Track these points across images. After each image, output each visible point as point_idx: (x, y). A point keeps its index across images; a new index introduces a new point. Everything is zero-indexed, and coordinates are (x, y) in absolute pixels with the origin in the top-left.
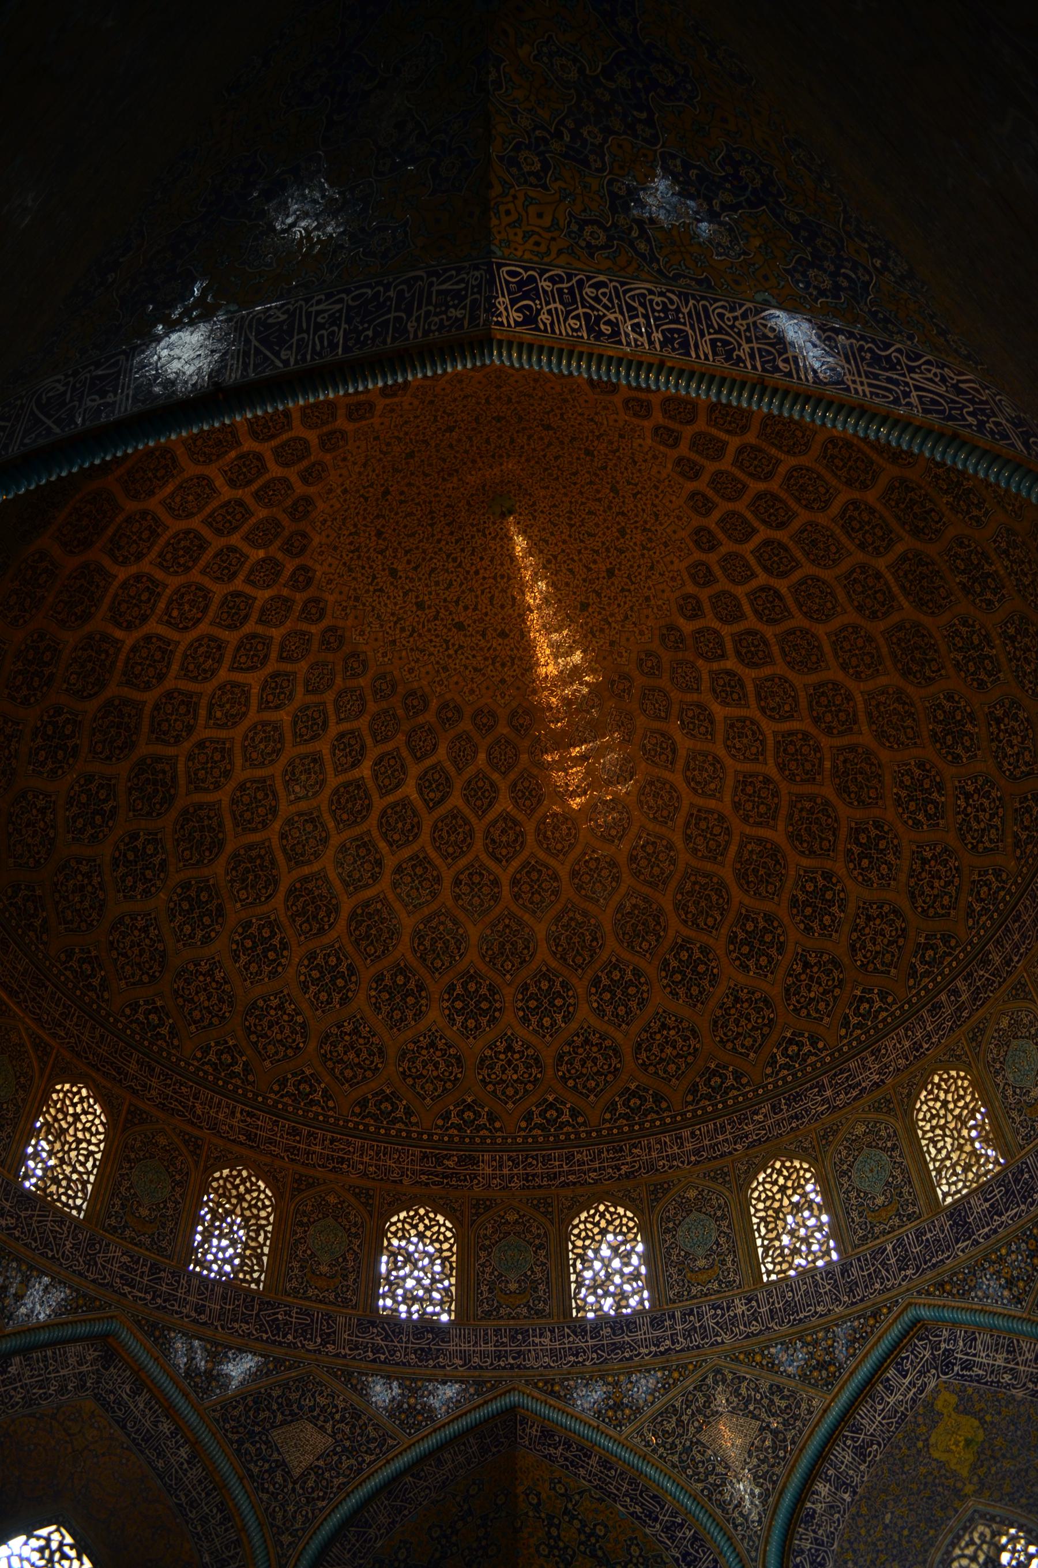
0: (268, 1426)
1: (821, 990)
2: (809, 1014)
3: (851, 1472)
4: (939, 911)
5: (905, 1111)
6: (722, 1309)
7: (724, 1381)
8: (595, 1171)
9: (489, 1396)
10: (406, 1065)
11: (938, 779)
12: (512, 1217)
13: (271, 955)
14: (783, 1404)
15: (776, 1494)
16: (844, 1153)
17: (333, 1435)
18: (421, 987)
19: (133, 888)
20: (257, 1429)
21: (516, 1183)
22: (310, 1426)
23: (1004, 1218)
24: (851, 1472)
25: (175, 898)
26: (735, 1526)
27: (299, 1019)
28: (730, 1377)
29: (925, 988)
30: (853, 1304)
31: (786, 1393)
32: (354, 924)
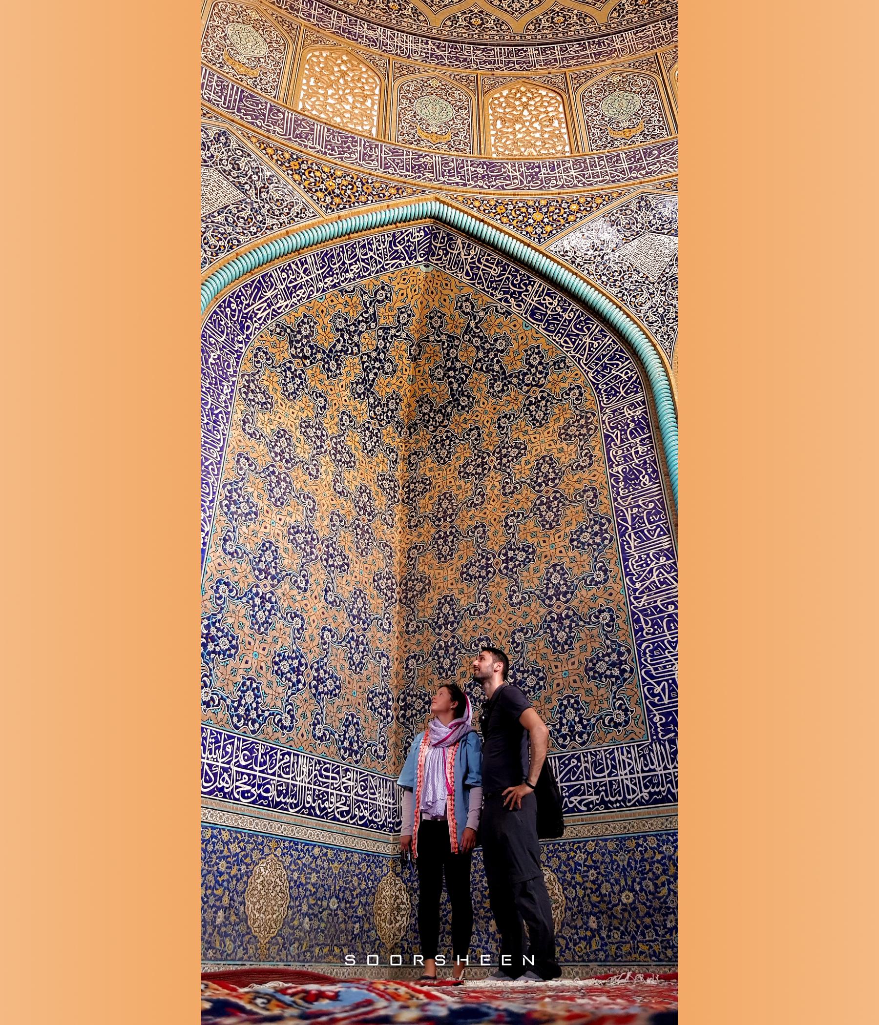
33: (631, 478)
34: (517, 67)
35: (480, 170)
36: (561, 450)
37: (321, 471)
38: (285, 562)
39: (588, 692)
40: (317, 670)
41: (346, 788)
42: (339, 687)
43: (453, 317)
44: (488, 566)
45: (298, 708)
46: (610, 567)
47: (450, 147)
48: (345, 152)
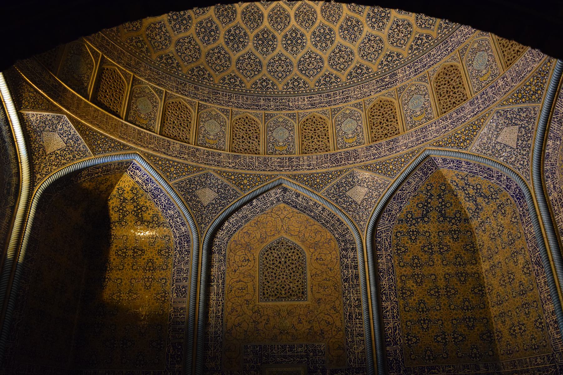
0: (344, 192)
3: (558, 132)
7: (501, 115)
9: (417, 155)
10: (362, 53)
12: (413, 88)
13: (299, 41)
15: (531, 151)
17: (368, 187)
18: (358, 22)
19: (238, 47)
20: (341, 194)
21: (412, 75)
22: (359, 187)
24: (558, 132)
25: (255, 42)
26: (519, 169)
27: (318, 57)
28: (502, 112)
31: (525, 110)
32: (324, 13)
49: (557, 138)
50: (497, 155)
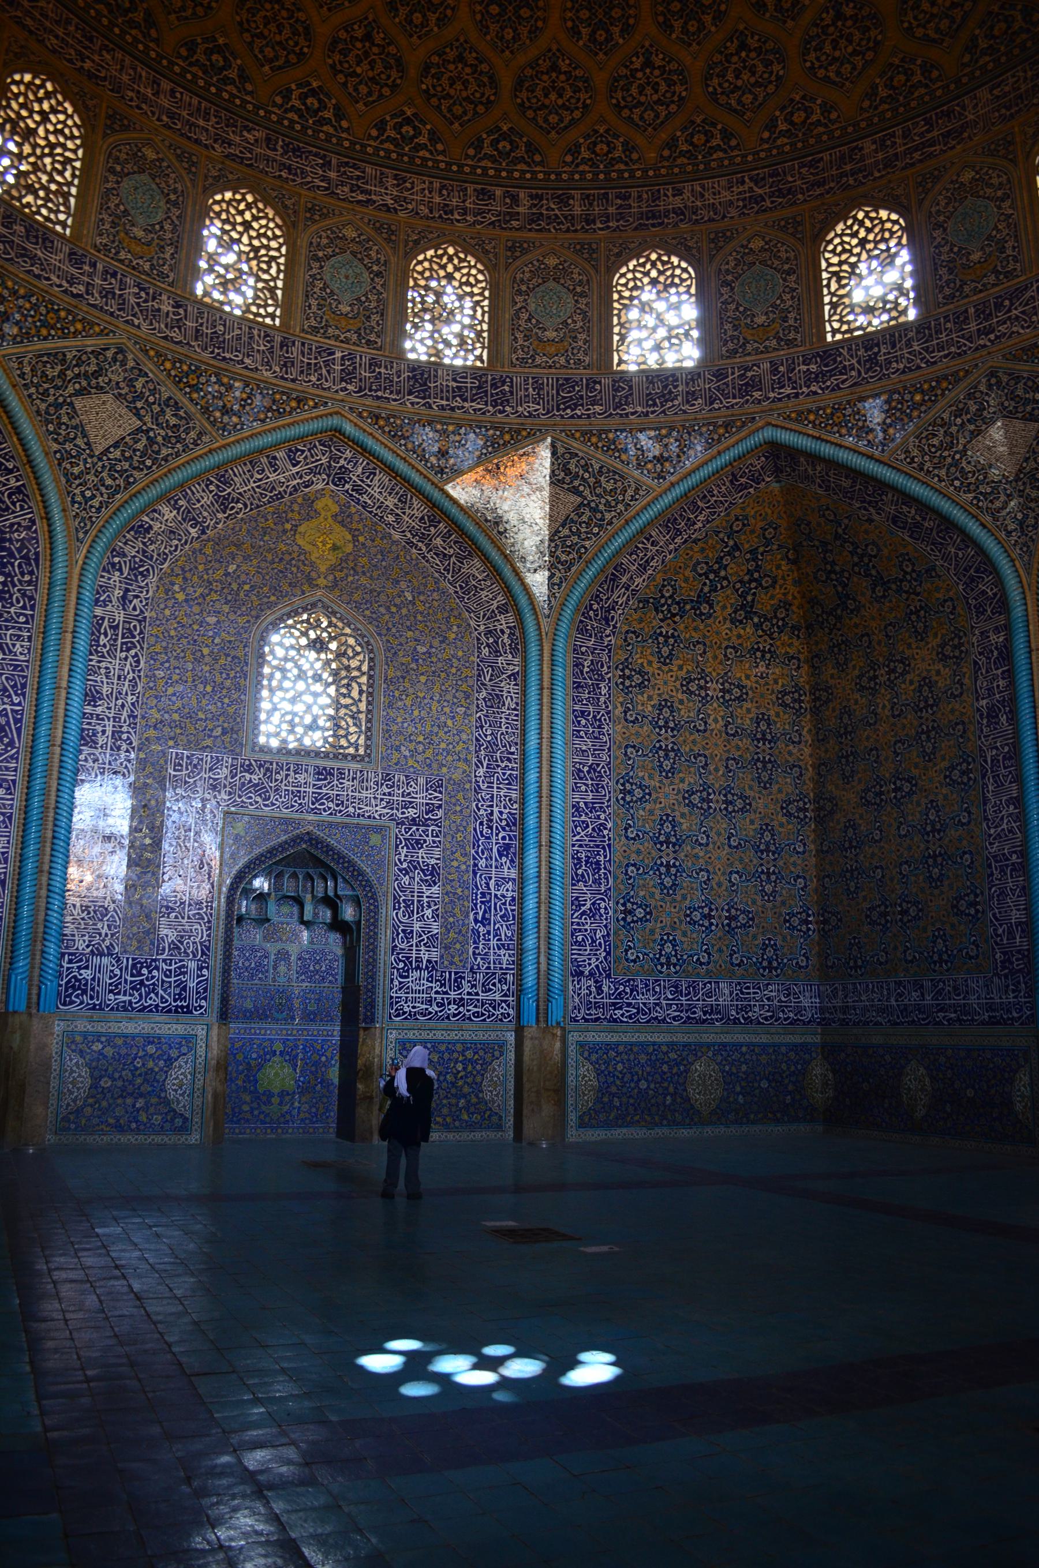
1: (370, 74)
2: (345, 84)
3: (205, 514)
4: (540, 121)
5: (406, 254)
6: (147, 294)
7: (123, 363)
8: (57, 37)
11: (631, 21)
14: (173, 421)
16: (325, 241)
23: (466, 405)
24: (205, 514)
26: (73, 502)
28: (131, 364)
29: (485, 169)
30: (282, 378)
31: (181, 413)
33: (992, 714)
34: (851, 182)
35: (813, 367)
36: (938, 672)
37: (710, 721)
38: (684, 827)
39: (953, 925)
40: (728, 911)
41: (768, 999)
42: (752, 919)
43: (819, 524)
44: (881, 793)
45: (713, 946)
46: (973, 810)
47: (779, 339)
48: (666, 401)
49: (190, 517)
50: (51, 428)
